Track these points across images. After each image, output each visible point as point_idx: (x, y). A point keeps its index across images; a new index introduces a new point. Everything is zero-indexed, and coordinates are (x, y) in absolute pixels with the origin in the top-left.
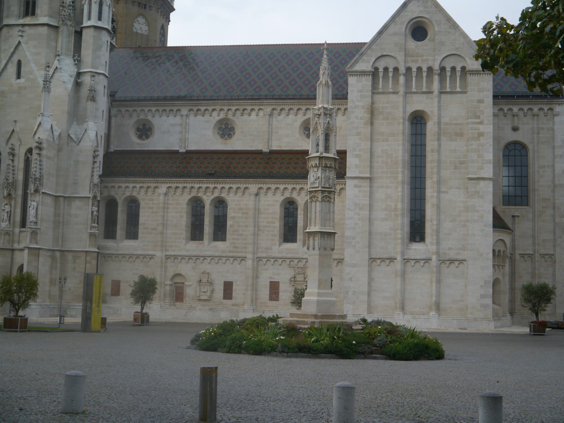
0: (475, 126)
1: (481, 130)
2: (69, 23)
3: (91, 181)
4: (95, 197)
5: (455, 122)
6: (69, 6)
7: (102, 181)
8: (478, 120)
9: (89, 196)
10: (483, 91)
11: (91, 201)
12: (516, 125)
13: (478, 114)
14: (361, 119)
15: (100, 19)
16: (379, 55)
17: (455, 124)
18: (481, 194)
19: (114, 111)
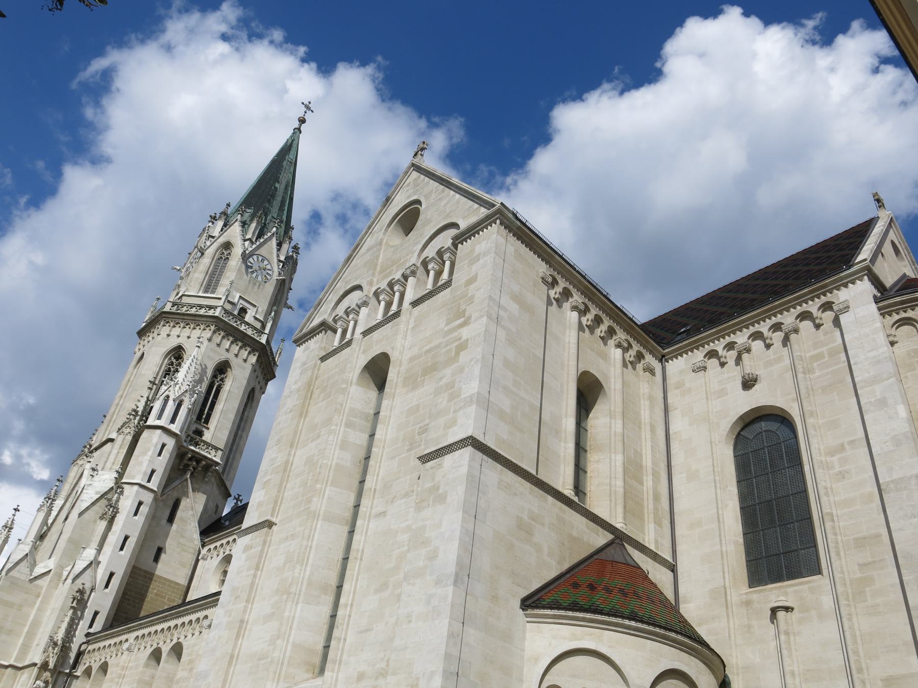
0: (455, 334)
1: (464, 338)
2: (128, 430)
3: (51, 638)
4: (44, 666)
5: (428, 347)
6: (134, 411)
7: (87, 643)
8: (462, 319)
9: (37, 662)
10: (479, 259)
11: (36, 669)
12: (748, 370)
13: (463, 307)
14: (291, 411)
15: (159, 417)
16: (341, 293)
17: (427, 352)
18: (440, 491)
19: (204, 551)
